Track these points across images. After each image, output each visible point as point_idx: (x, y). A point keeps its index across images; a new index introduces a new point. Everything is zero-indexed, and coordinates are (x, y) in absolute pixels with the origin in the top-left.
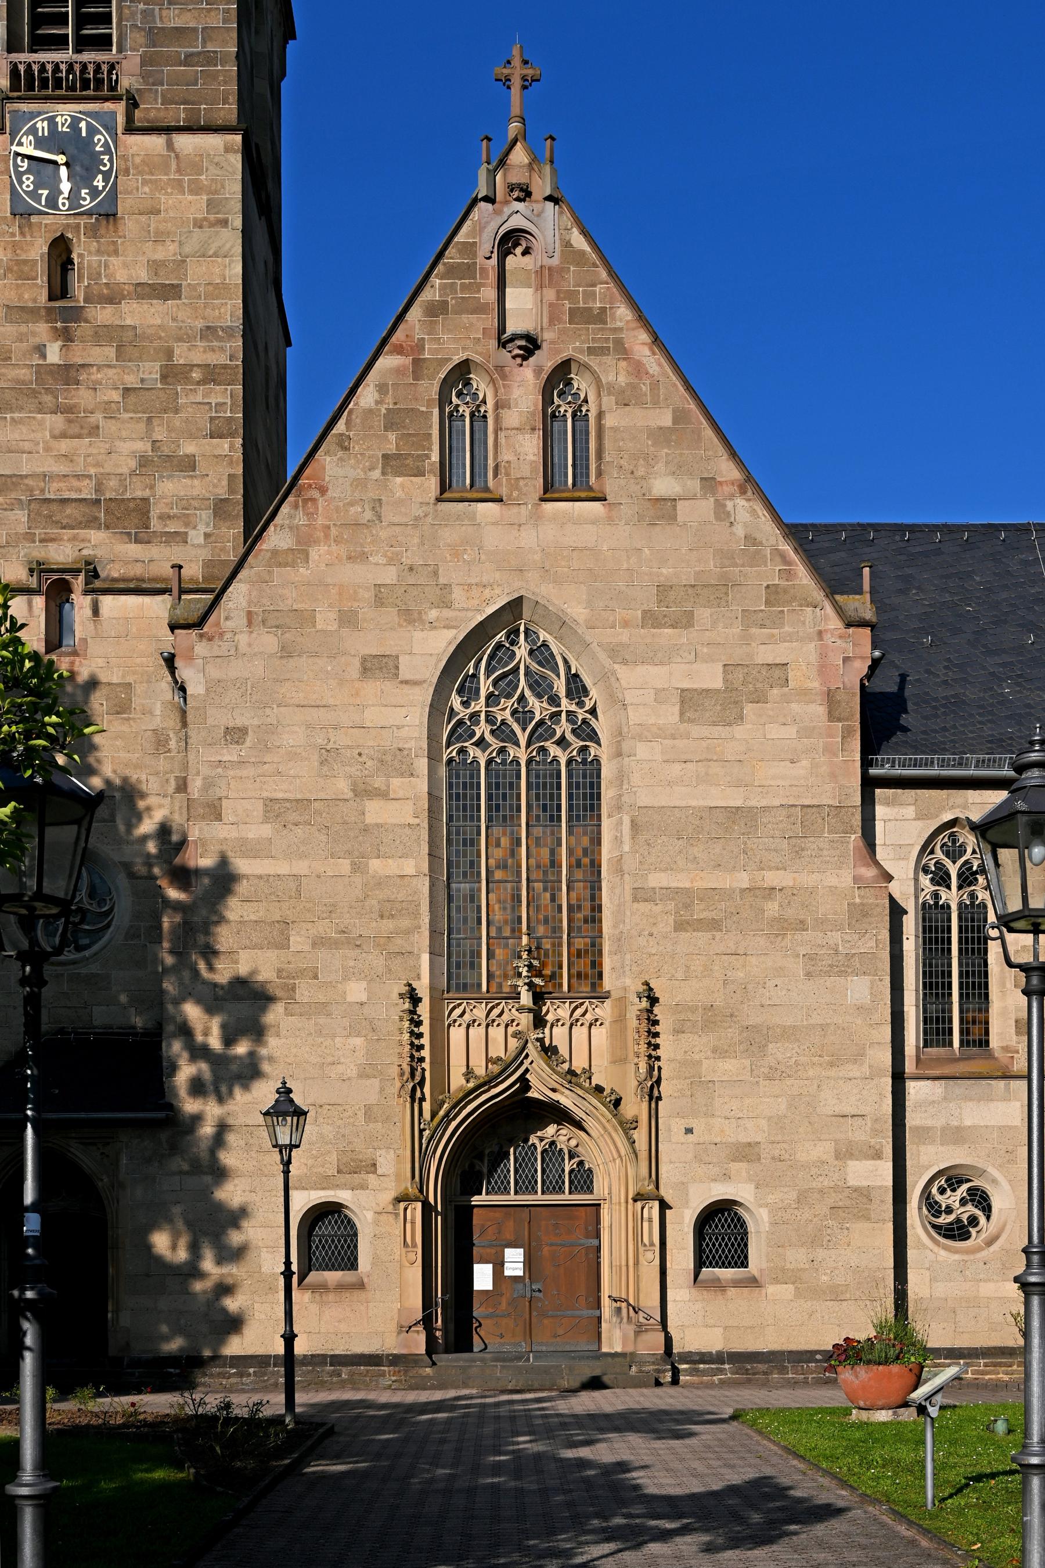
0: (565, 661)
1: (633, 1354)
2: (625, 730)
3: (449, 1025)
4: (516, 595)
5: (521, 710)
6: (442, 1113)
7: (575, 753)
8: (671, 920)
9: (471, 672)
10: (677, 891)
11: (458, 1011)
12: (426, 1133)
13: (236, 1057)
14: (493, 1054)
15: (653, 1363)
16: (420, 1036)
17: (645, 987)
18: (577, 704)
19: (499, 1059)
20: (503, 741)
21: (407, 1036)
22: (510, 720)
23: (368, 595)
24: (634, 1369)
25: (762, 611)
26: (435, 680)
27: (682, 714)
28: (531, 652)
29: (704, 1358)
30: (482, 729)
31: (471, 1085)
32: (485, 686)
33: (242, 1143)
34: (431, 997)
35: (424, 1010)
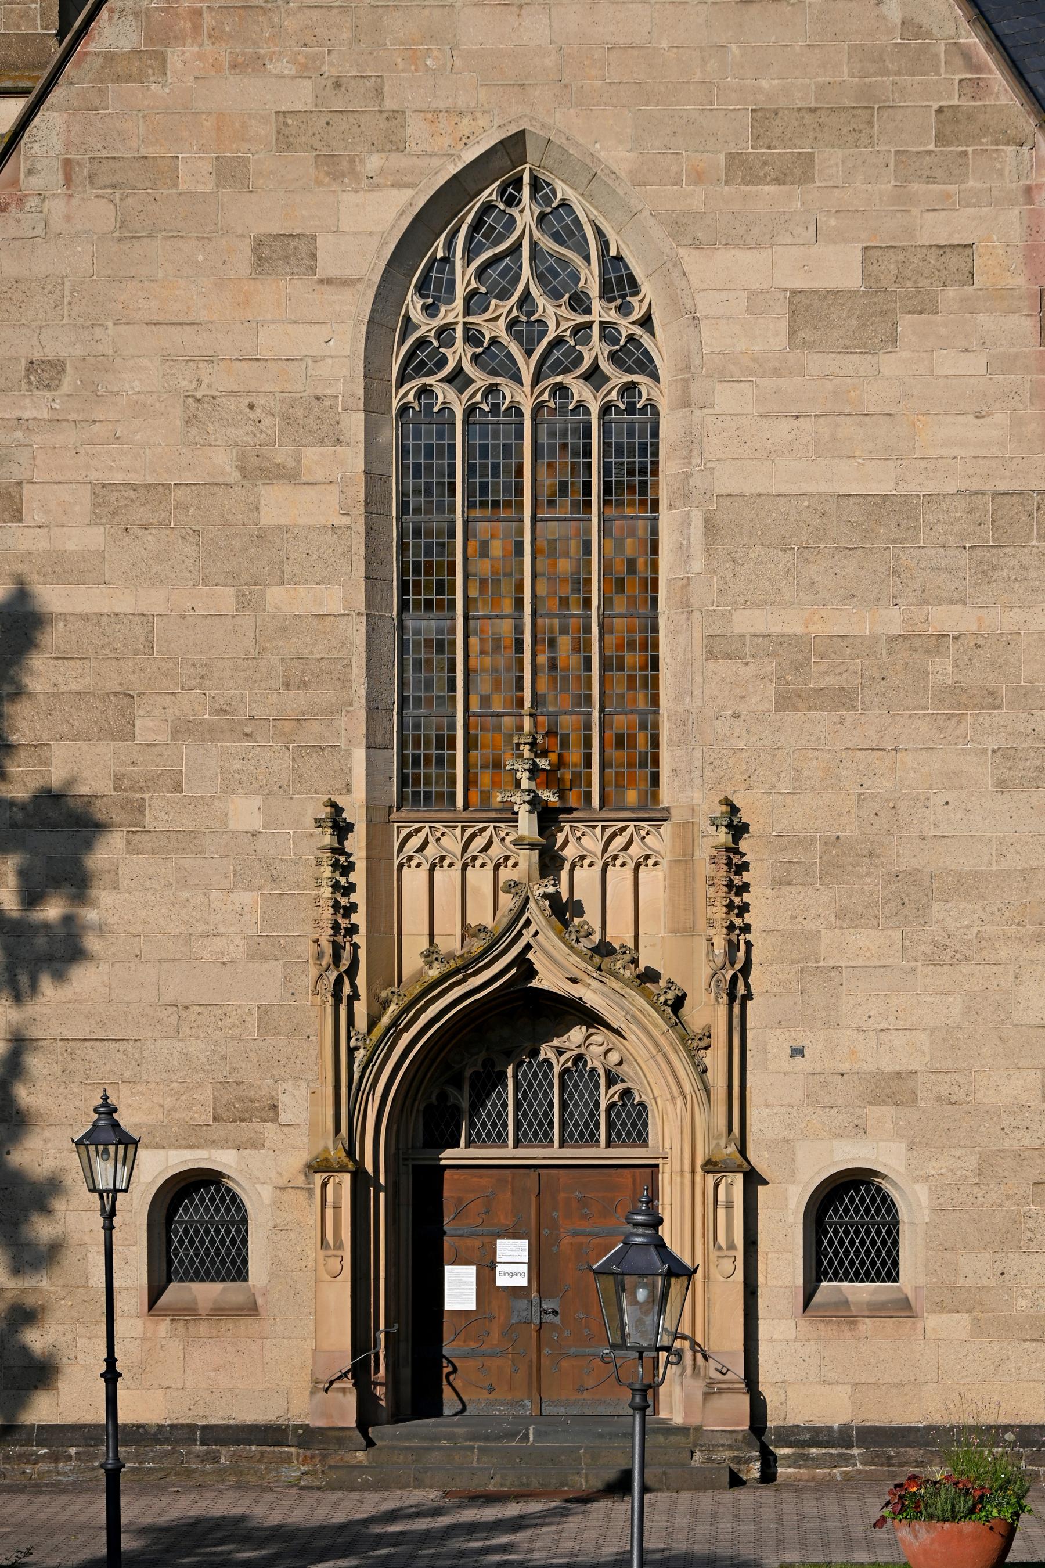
0: (599, 233)
1: (698, 1429)
2: (697, 361)
3: (401, 866)
4: (513, 129)
5: (524, 318)
6: (386, 1020)
7: (614, 395)
8: (771, 689)
9: (440, 254)
10: (782, 640)
11: (416, 842)
12: (360, 1055)
13: (46, 926)
14: (472, 921)
15: (731, 1447)
16: (351, 888)
17: (724, 808)
18: (619, 308)
19: (482, 929)
20: (494, 373)
21: (327, 892)
22: (505, 338)
23: (267, 130)
24: (698, 1456)
25: (929, 153)
26: (377, 278)
27: (792, 333)
28: (542, 218)
29: (818, 1436)
30: (459, 353)
31: (434, 973)
32: (464, 278)
33: (57, 1069)
34: (369, 823)
35: (356, 844)
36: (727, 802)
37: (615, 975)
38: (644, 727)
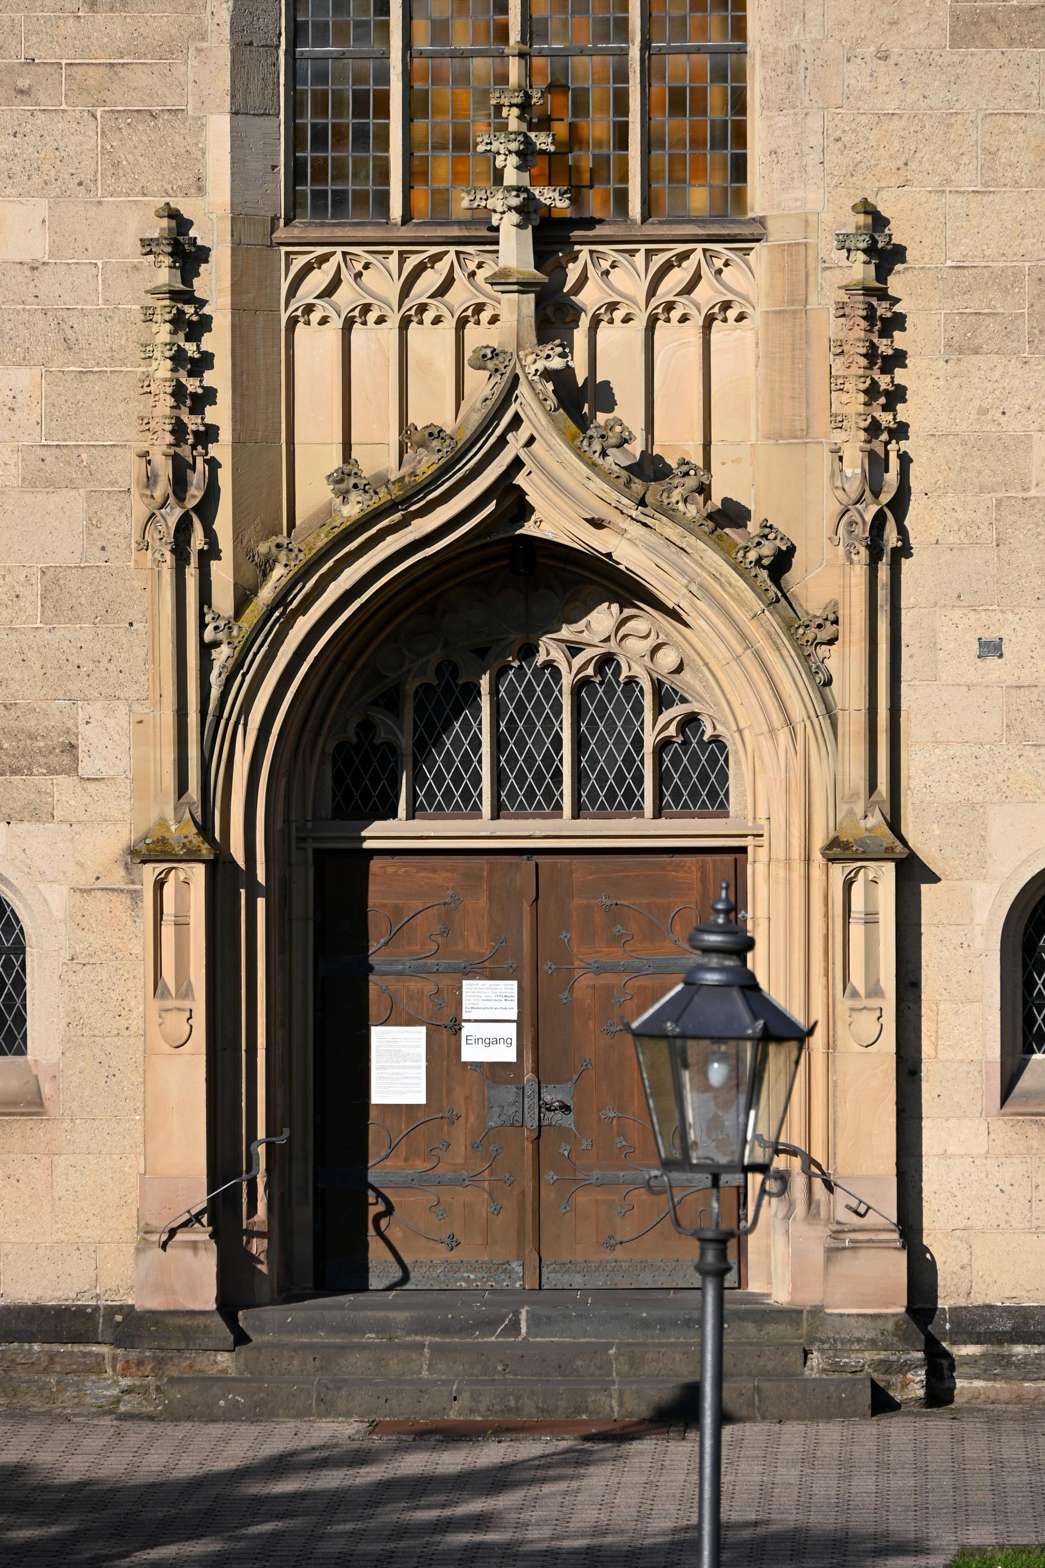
6: (266, 594)
12: (222, 655)
14: (418, 418)
16: (204, 363)
17: (862, 219)
19: (435, 433)
21: (163, 369)
31: (352, 510)
34: (237, 246)
36: (868, 209)
37: (669, 513)
38: (719, 75)
